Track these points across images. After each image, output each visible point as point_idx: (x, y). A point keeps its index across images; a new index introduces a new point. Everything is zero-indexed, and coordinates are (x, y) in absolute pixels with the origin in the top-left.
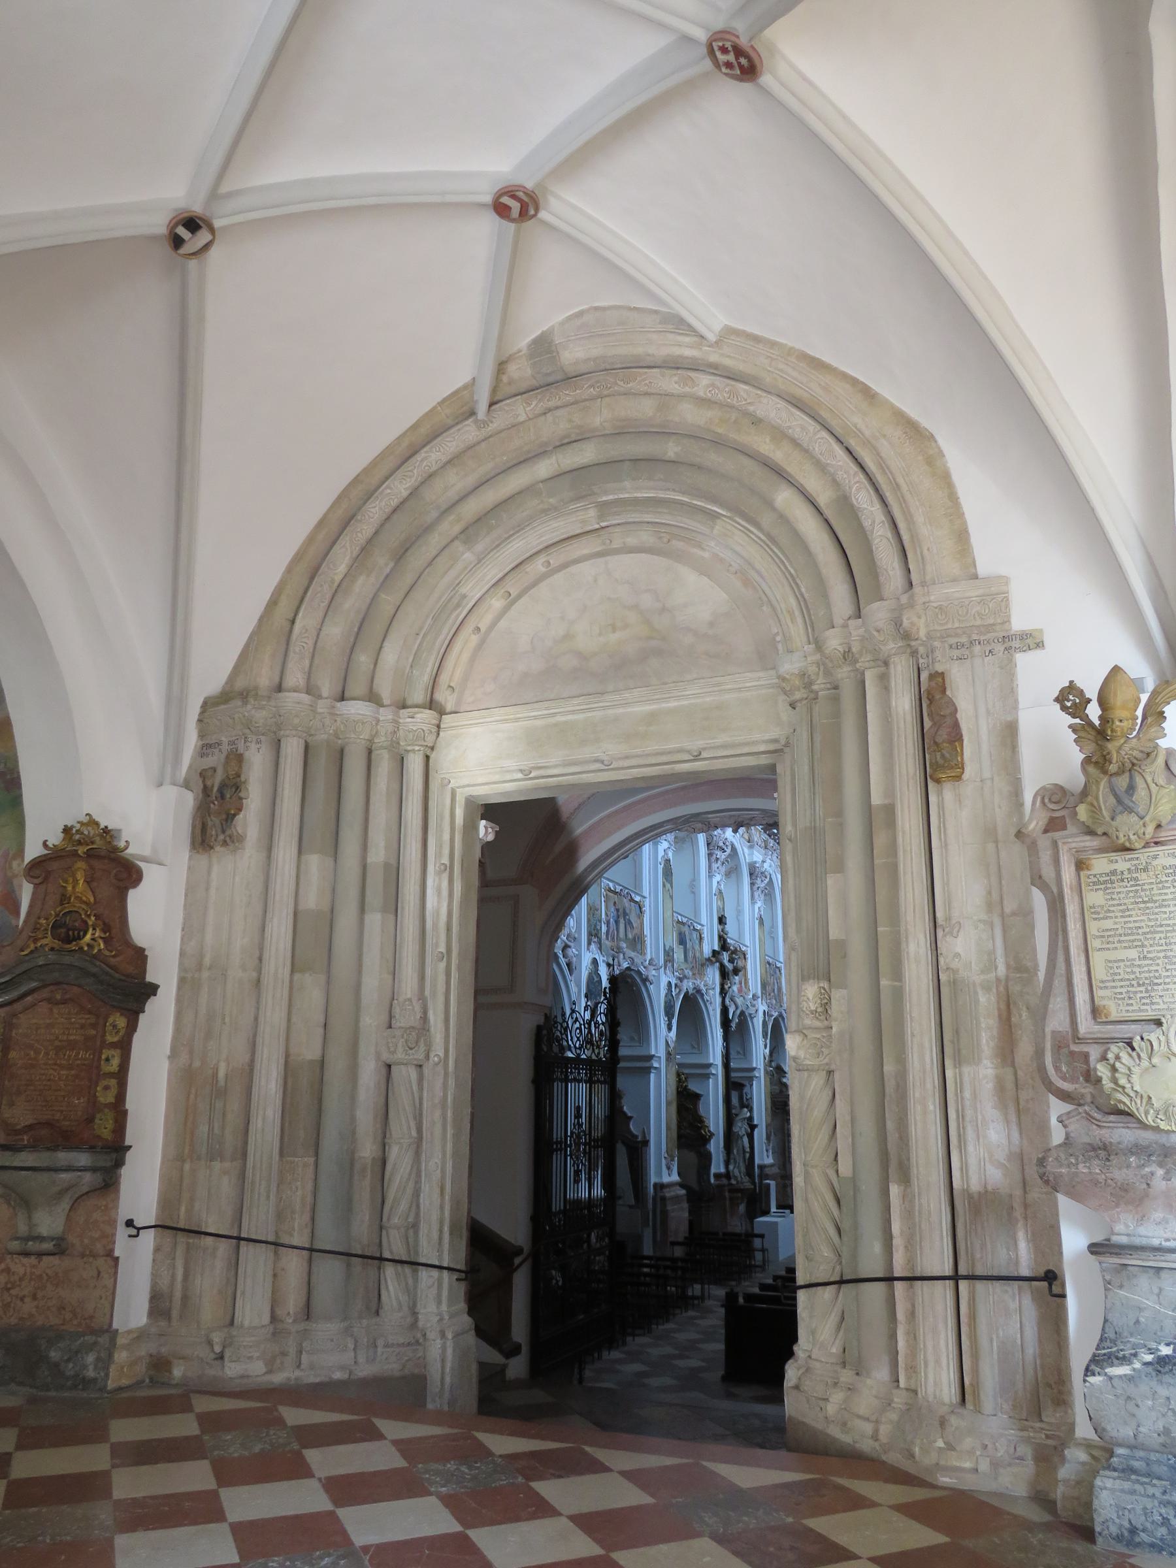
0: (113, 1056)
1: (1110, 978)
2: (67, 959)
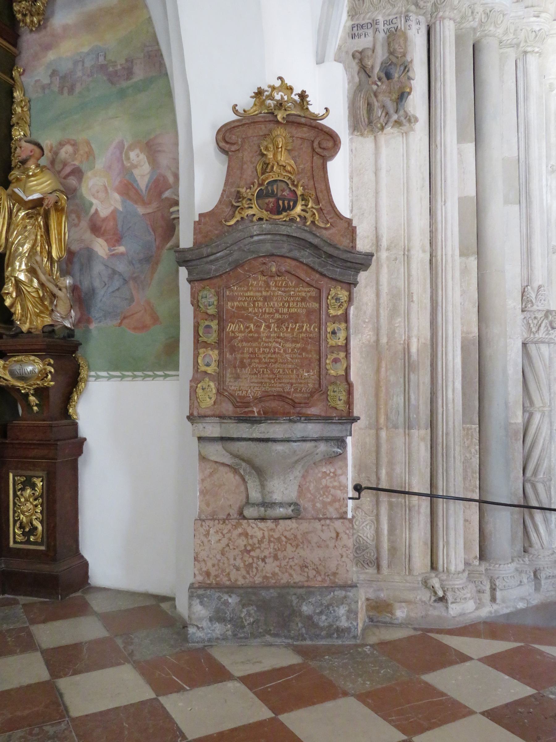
0: (339, 329)
2: (284, 230)
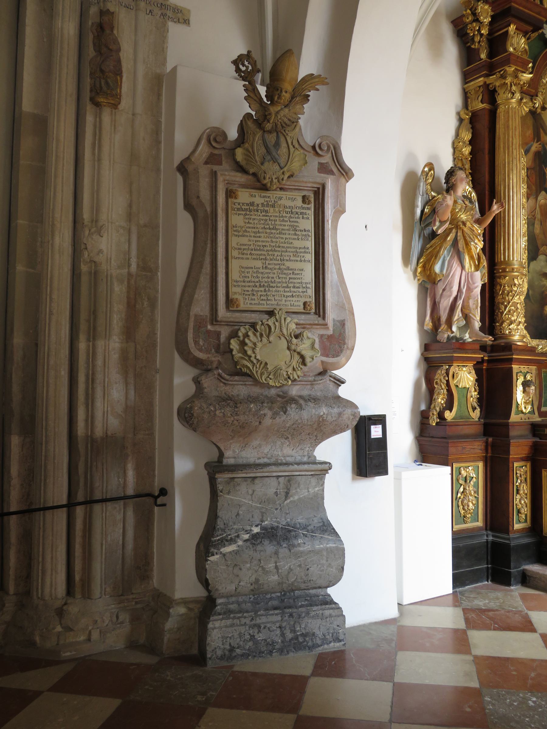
1: (242, 279)
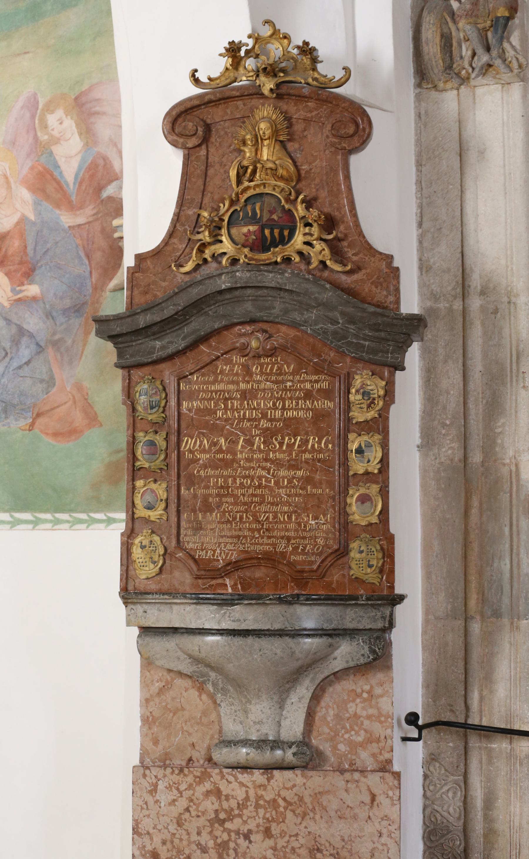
0: (369, 445)
